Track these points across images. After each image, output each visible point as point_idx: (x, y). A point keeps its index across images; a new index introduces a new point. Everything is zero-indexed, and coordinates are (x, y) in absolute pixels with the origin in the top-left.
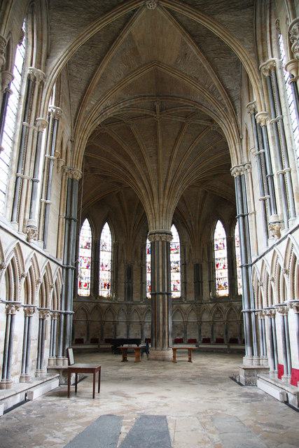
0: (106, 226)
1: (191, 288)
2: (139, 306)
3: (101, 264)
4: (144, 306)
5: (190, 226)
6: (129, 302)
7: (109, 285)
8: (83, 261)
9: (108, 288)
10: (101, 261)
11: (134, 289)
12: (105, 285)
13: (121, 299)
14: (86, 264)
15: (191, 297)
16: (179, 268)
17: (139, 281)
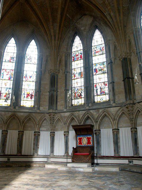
0: (33, 44)
1: (120, 87)
2: (62, 114)
3: (24, 75)
4: (67, 114)
5: (110, 20)
6: (51, 111)
7: (32, 95)
8: (5, 73)
9: (31, 98)
10: (25, 73)
11: (59, 98)
12: (28, 95)
13: (45, 108)
14: (8, 76)
15: (121, 98)
16: (106, 69)
17: (63, 89)
